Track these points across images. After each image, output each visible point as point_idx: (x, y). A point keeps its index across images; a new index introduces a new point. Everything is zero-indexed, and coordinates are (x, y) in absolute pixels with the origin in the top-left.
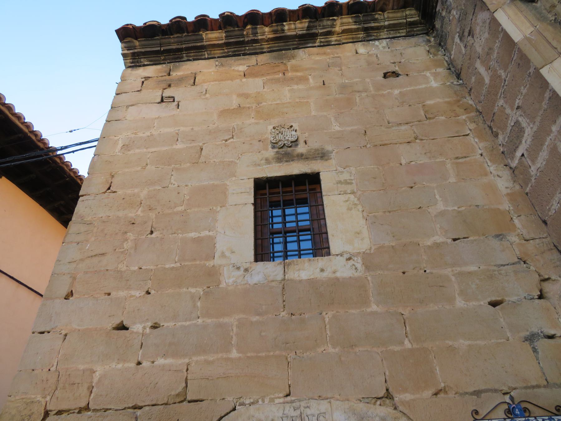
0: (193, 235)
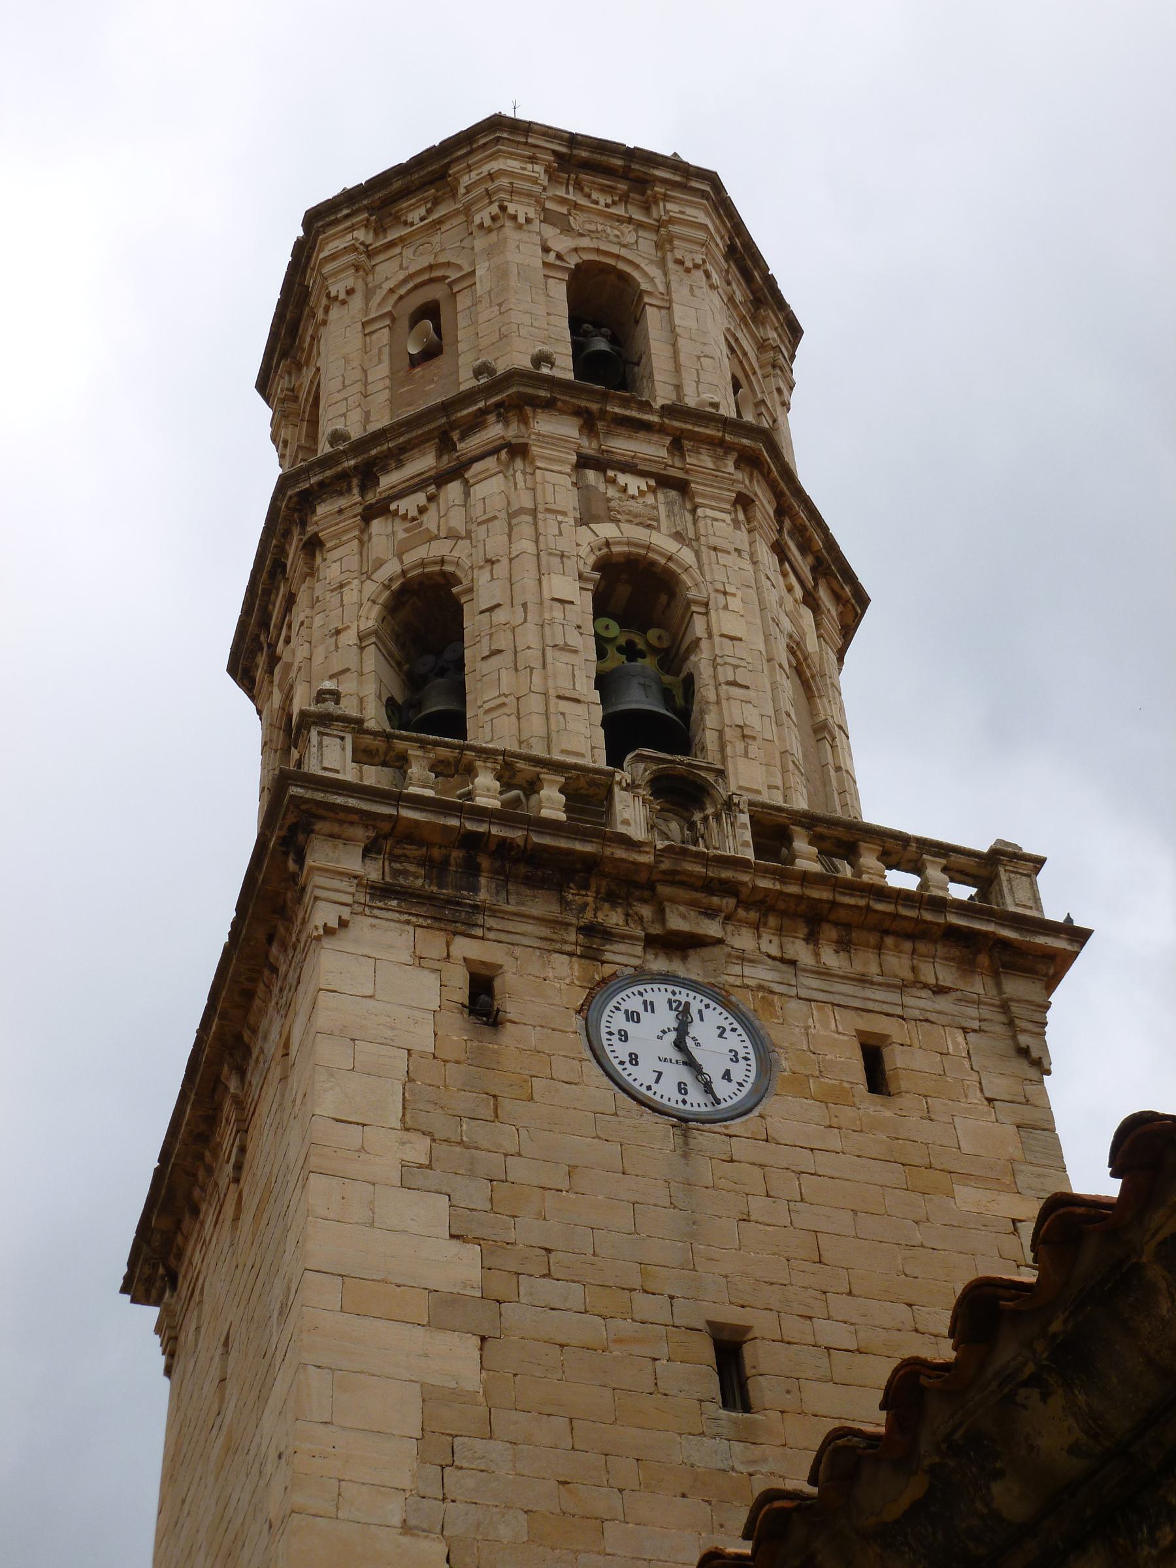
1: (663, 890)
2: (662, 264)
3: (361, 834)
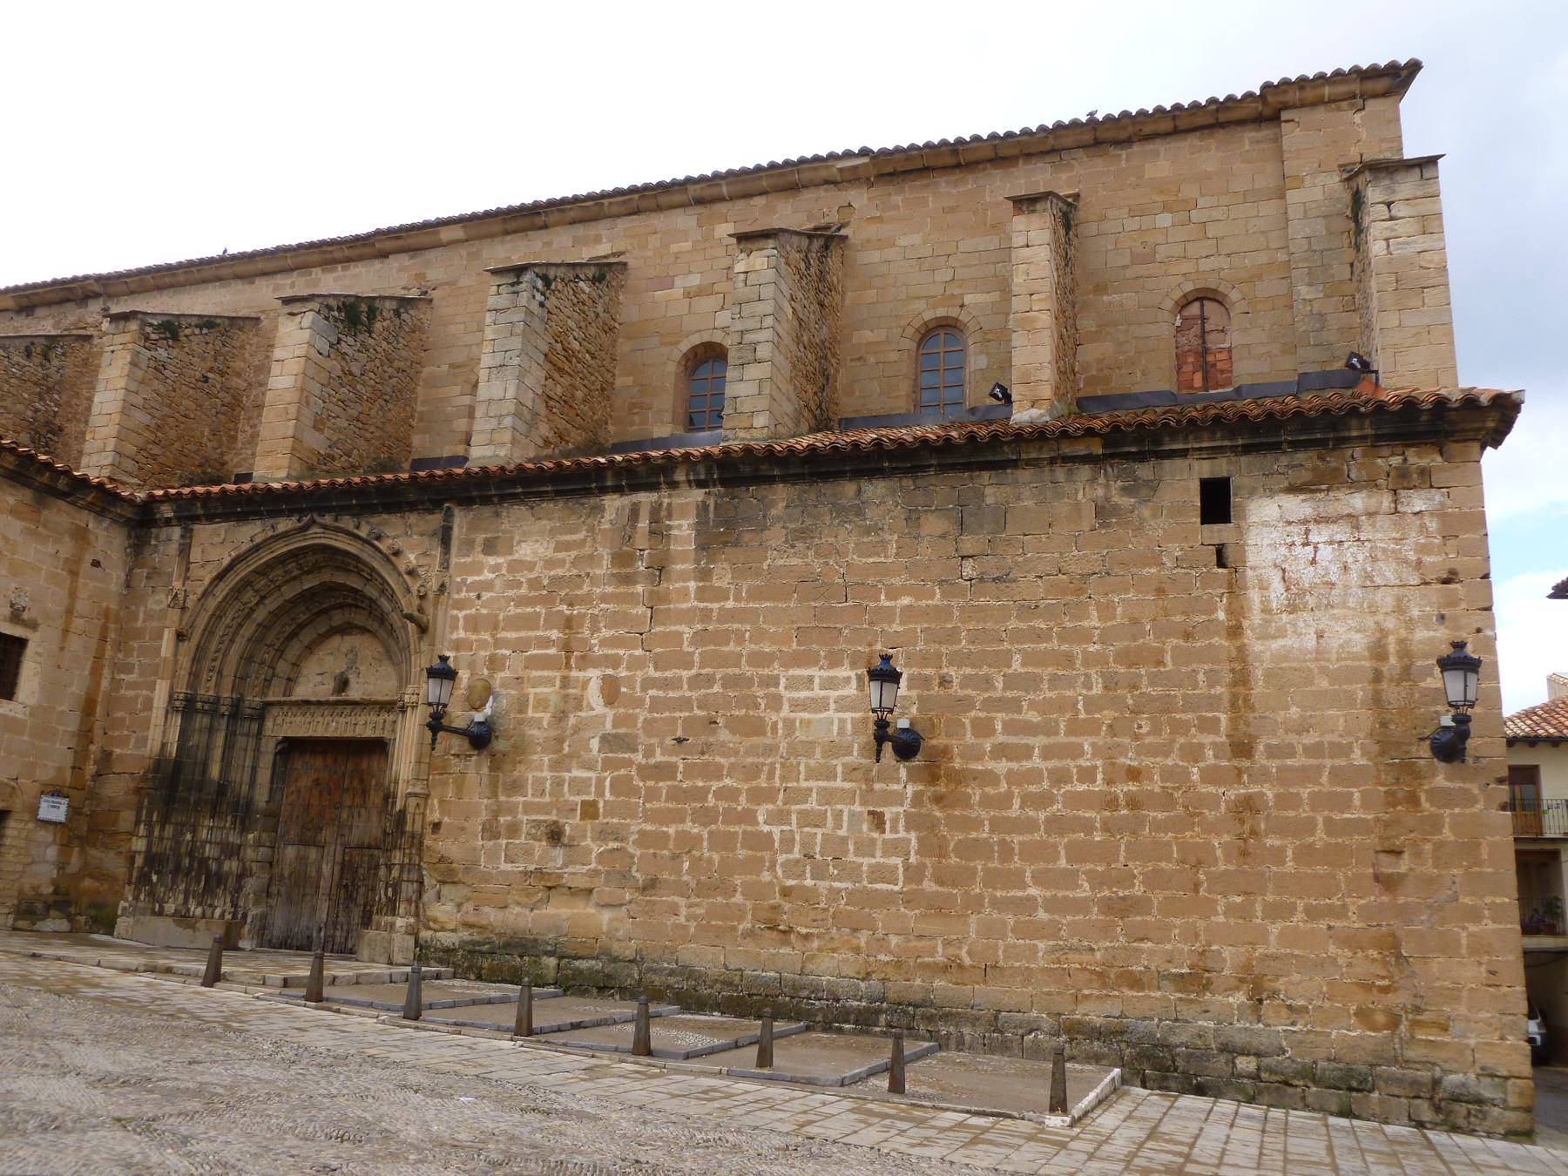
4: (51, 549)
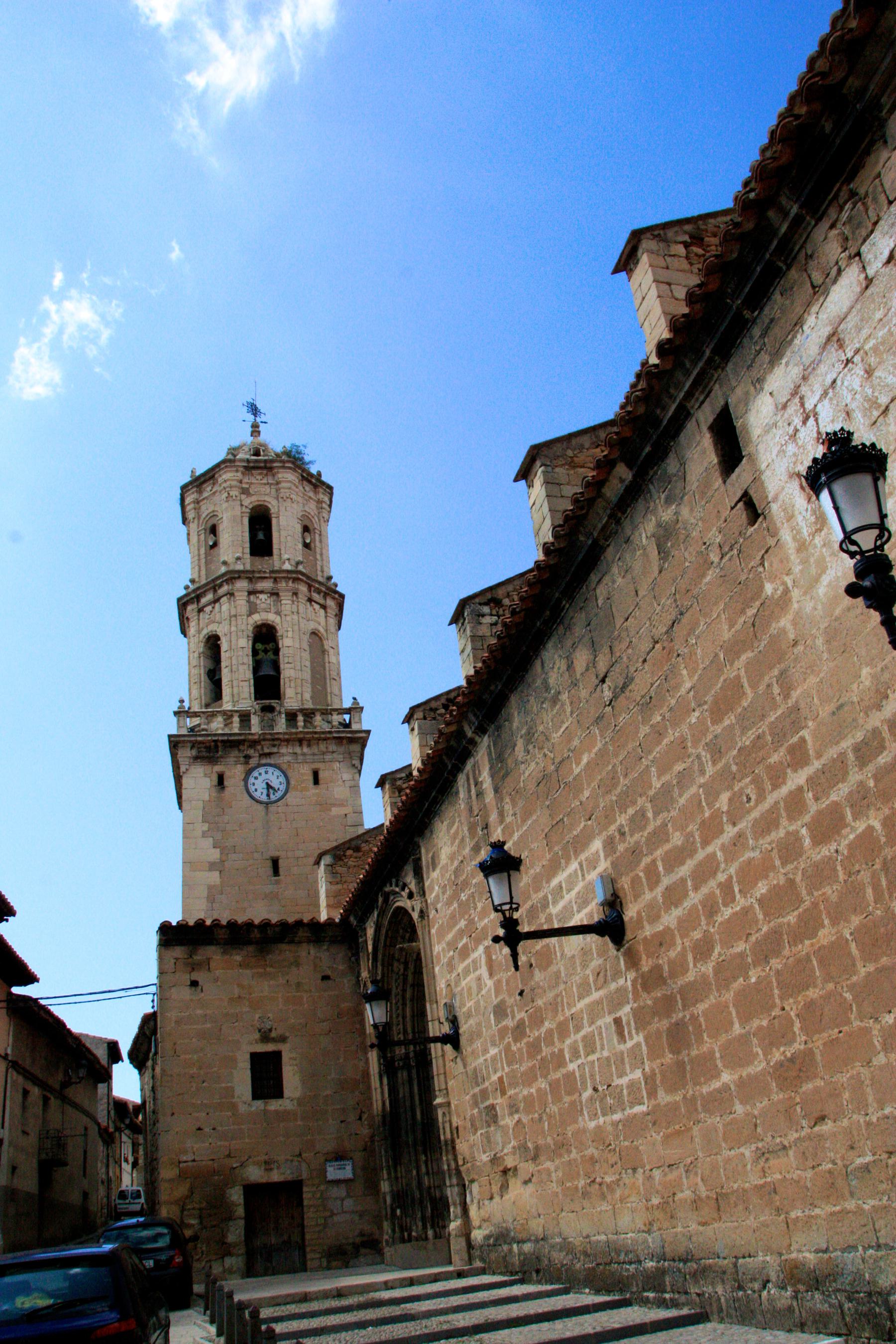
0: (223, 1085)
1: (263, 743)
2: (277, 498)
3: (189, 745)
4: (282, 981)
